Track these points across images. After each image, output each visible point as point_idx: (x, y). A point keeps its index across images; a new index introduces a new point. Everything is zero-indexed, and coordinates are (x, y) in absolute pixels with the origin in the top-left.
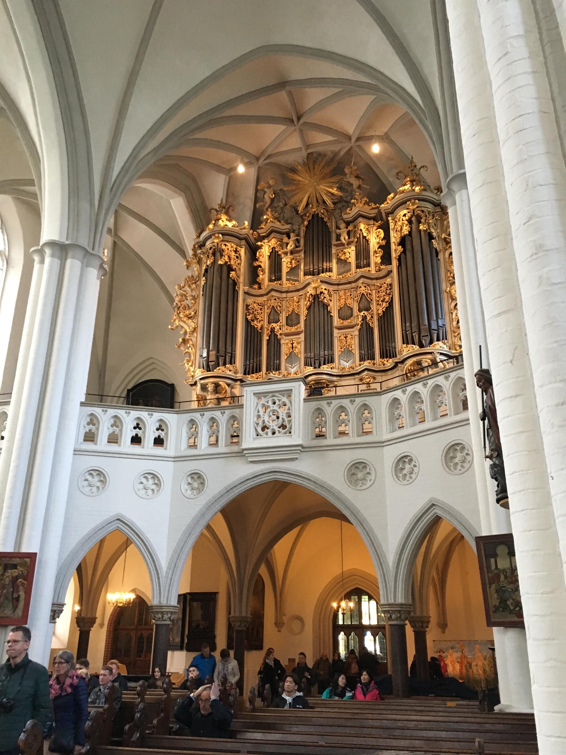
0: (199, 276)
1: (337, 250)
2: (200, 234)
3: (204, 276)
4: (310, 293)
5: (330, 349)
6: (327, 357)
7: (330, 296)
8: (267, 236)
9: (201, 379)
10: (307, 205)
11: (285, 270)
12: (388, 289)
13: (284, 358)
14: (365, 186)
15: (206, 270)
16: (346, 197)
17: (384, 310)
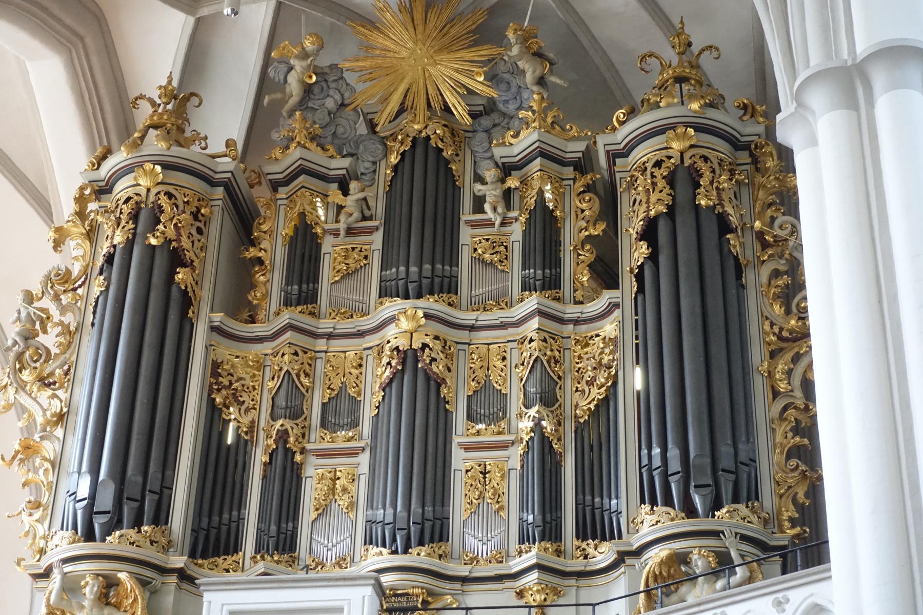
0: (86, 273)
1: (473, 237)
2: (104, 157)
3: (101, 273)
4: (394, 343)
5: (438, 503)
6: (428, 524)
8: (287, 181)
9: (66, 561)
10: (401, 111)
11: (327, 274)
12: (607, 351)
13: (308, 513)
14: (554, 79)
15: (109, 259)
16: (506, 102)
17: (592, 406)
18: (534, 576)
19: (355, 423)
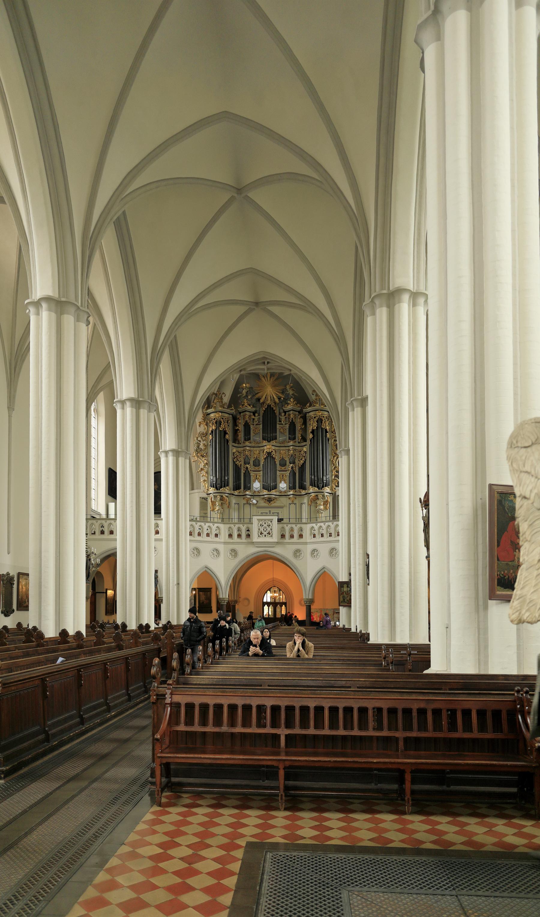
7: (276, 453)
14: (296, 394)
15: (212, 432)
18: (292, 496)
19: (259, 465)
